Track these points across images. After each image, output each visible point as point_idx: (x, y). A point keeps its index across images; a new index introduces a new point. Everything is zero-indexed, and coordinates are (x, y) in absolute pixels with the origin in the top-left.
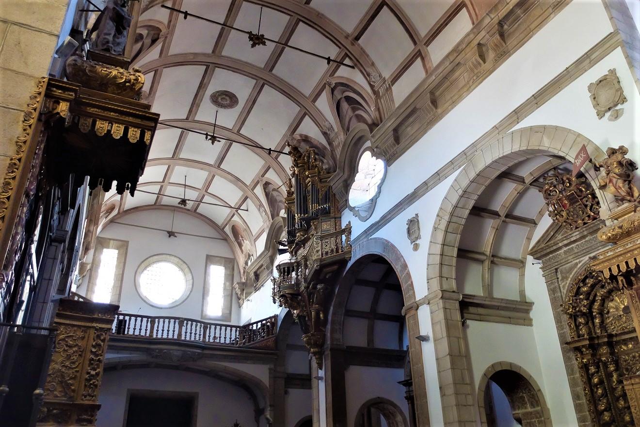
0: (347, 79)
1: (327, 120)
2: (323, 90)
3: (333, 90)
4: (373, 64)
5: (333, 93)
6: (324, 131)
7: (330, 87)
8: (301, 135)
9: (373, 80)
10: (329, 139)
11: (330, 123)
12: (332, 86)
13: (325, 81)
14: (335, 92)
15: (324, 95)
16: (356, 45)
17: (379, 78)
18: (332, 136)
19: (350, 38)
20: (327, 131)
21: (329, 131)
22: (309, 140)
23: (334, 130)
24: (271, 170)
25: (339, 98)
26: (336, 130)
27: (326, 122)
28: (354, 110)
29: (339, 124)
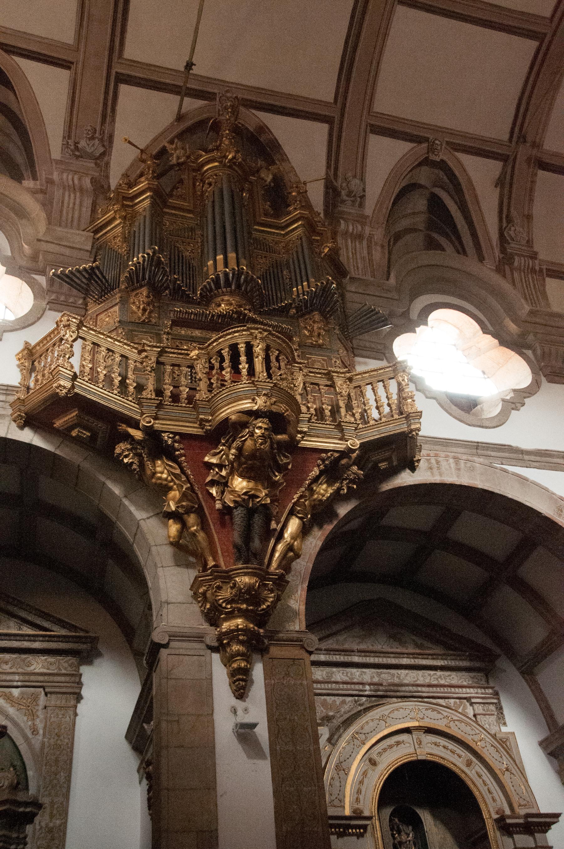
0: (470, 181)
1: (362, 179)
2: (411, 141)
3: (426, 162)
4: (529, 217)
5: (420, 164)
6: (335, 183)
7: (428, 153)
8: (263, 129)
9: (512, 233)
10: (335, 206)
11: (364, 190)
12: (432, 157)
13: (431, 137)
14: (424, 168)
15: (404, 147)
16: (531, 170)
17: (524, 242)
18: (347, 208)
19: (535, 152)
20: (343, 193)
21: (349, 194)
22: (276, 157)
23: (361, 205)
24: (64, 75)
25: (422, 182)
26: (368, 210)
27: (357, 181)
28: (431, 225)
29: (385, 212)
